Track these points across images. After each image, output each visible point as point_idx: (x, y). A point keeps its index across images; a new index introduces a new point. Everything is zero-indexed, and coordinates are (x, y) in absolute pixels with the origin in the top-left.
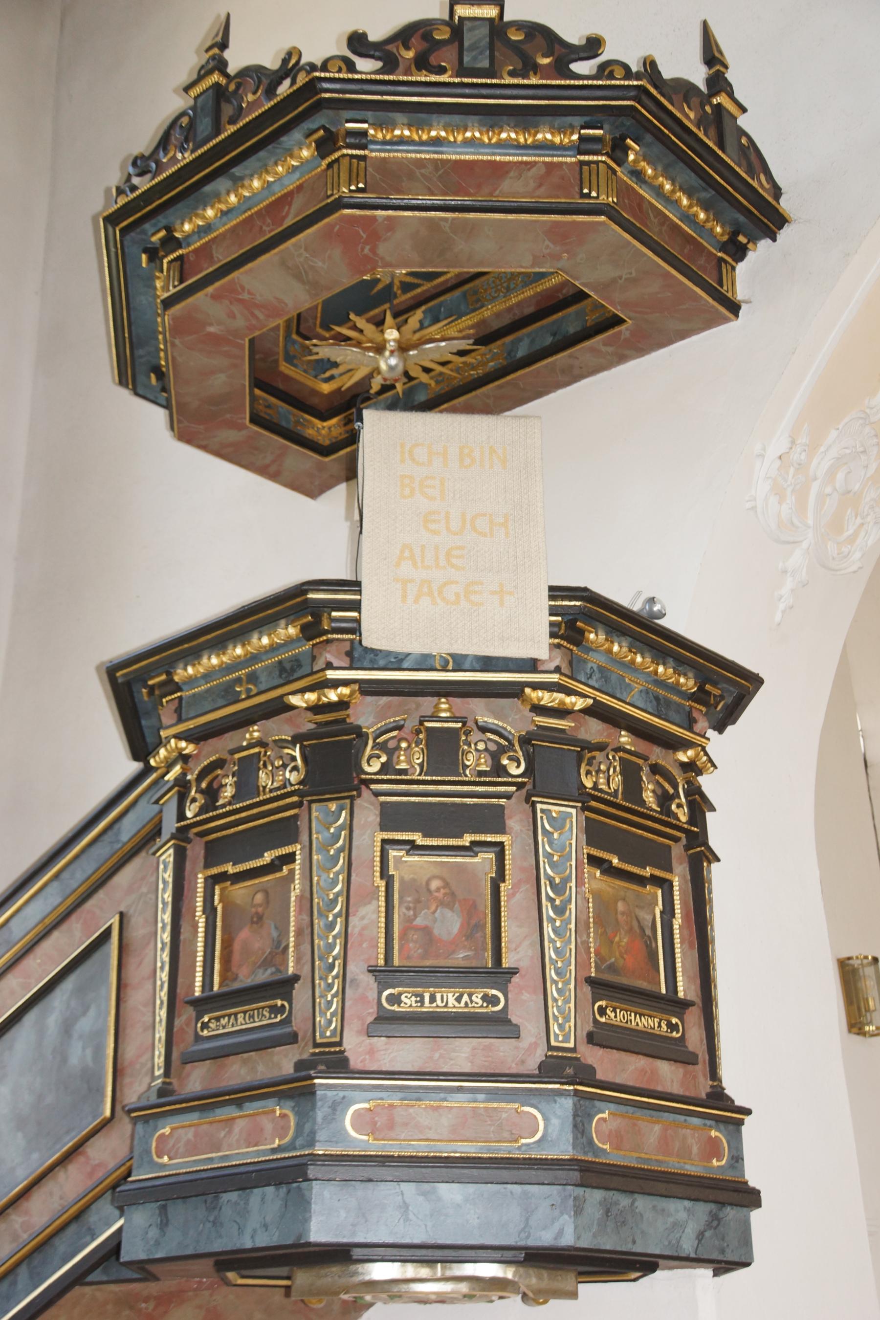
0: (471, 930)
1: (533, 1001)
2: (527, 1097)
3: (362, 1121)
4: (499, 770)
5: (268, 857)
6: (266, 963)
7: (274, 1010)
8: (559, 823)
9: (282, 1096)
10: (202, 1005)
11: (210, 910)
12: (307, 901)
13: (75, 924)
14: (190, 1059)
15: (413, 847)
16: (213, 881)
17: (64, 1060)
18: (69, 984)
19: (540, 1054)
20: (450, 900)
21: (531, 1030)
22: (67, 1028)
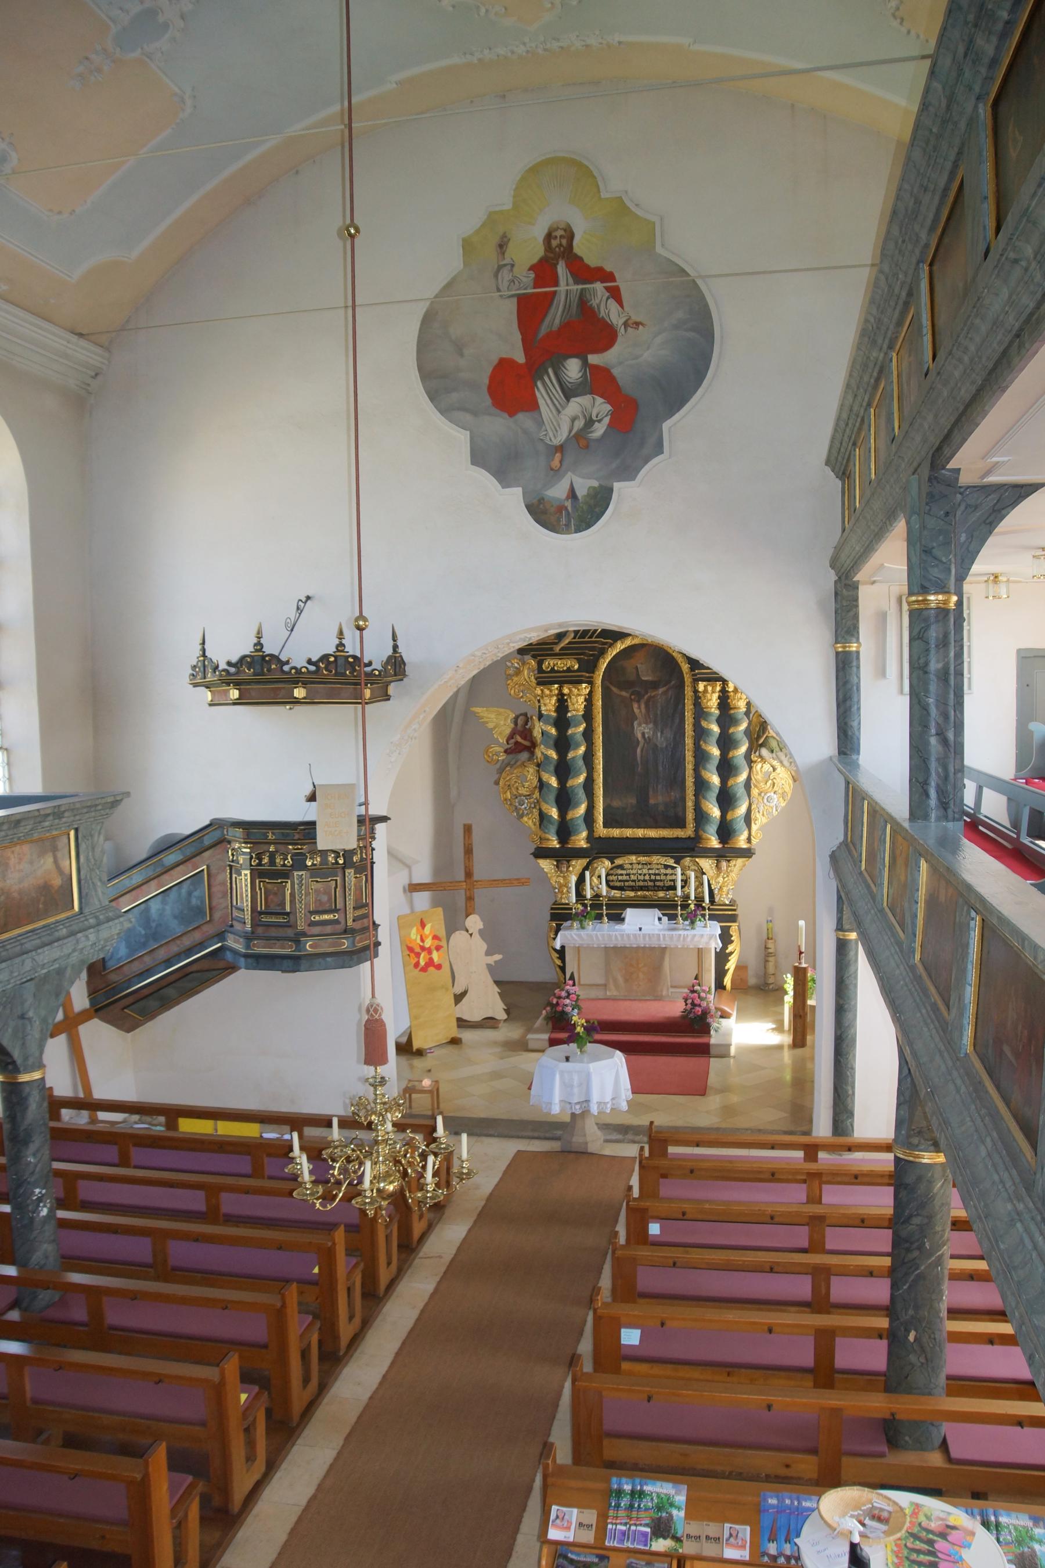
0: (330, 899)
1: (343, 915)
2: (344, 938)
3: (310, 946)
4: (337, 863)
5: (279, 881)
6: (279, 905)
7: (284, 919)
8: (350, 874)
9: (291, 941)
10: (261, 913)
11: (260, 889)
12: (292, 895)
13: (189, 865)
14: (258, 925)
15: (317, 881)
16: (260, 882)
17: (189, 902)
18: (188, 882)
19: (344, 927)
20: (325, 893)
21: (343, 922)
22: (190, 894)
